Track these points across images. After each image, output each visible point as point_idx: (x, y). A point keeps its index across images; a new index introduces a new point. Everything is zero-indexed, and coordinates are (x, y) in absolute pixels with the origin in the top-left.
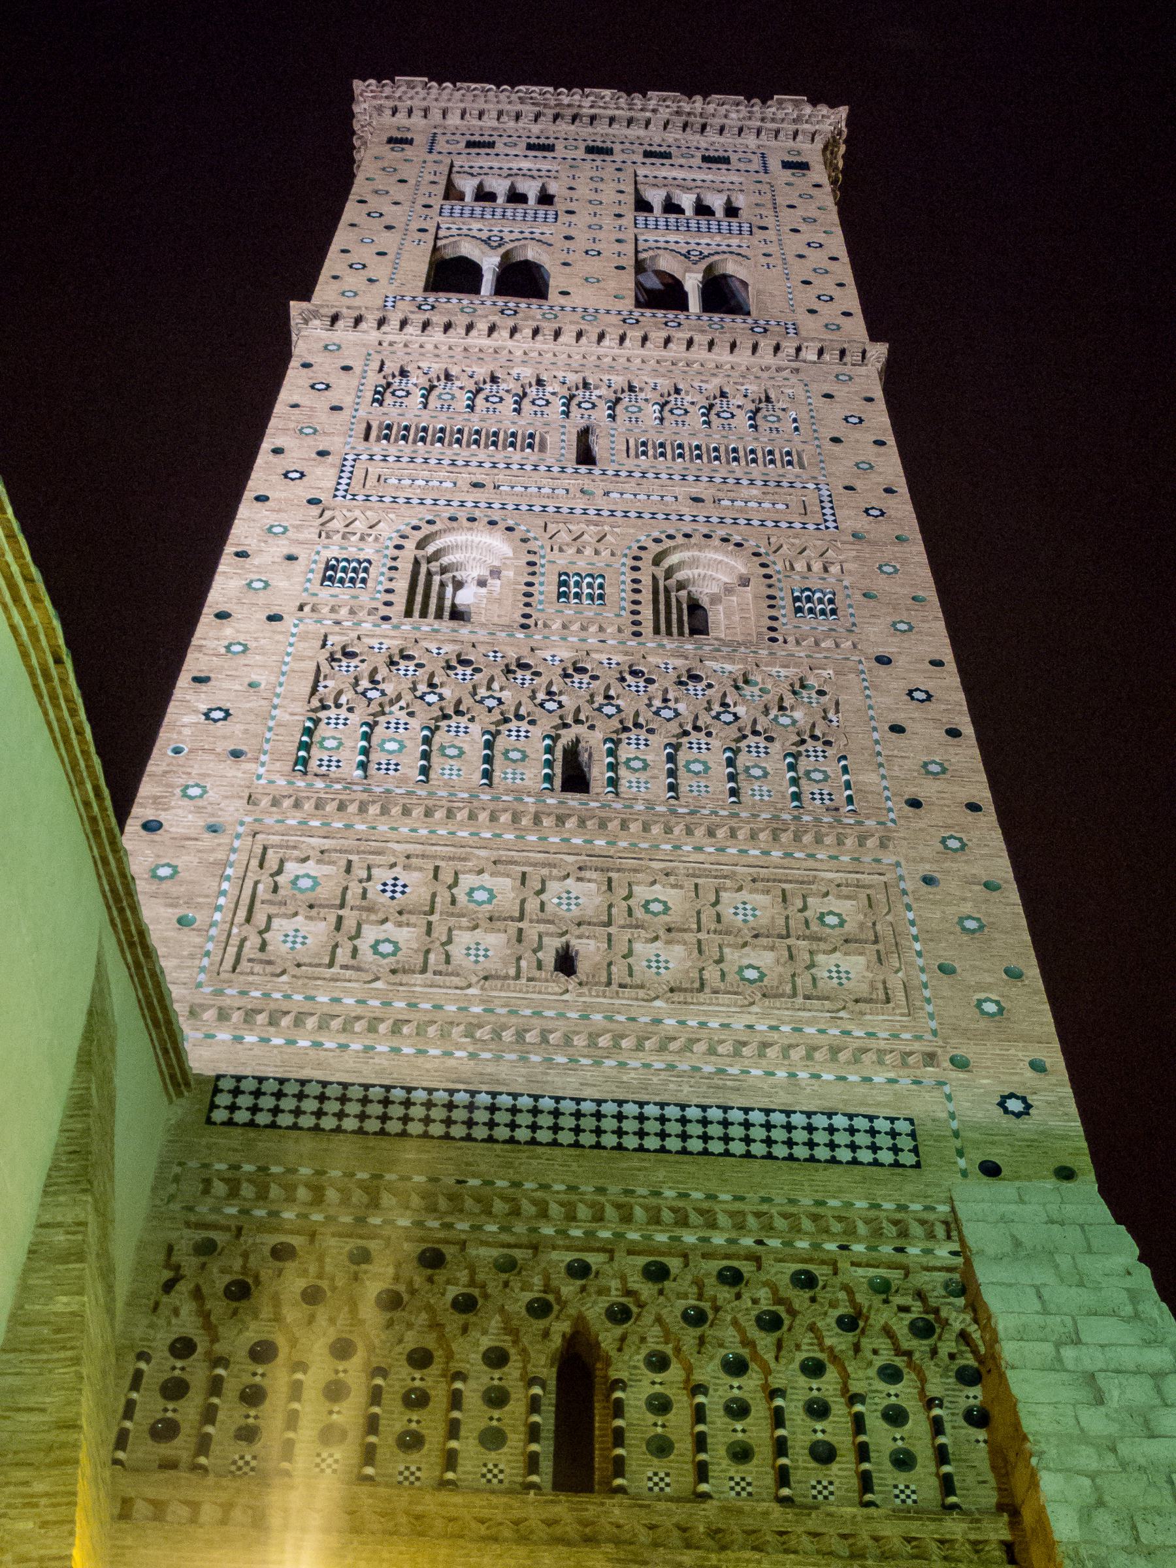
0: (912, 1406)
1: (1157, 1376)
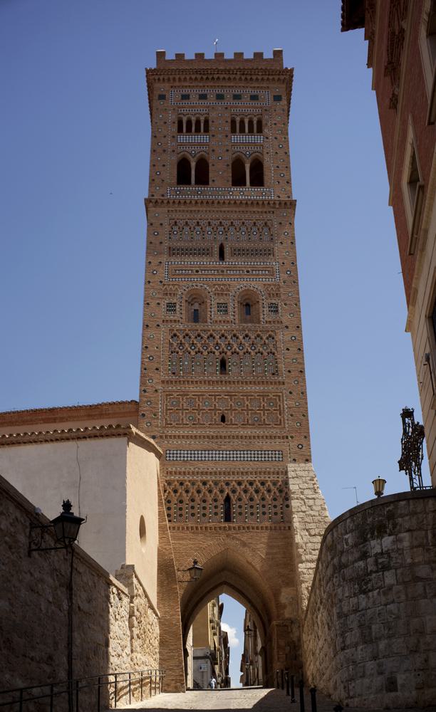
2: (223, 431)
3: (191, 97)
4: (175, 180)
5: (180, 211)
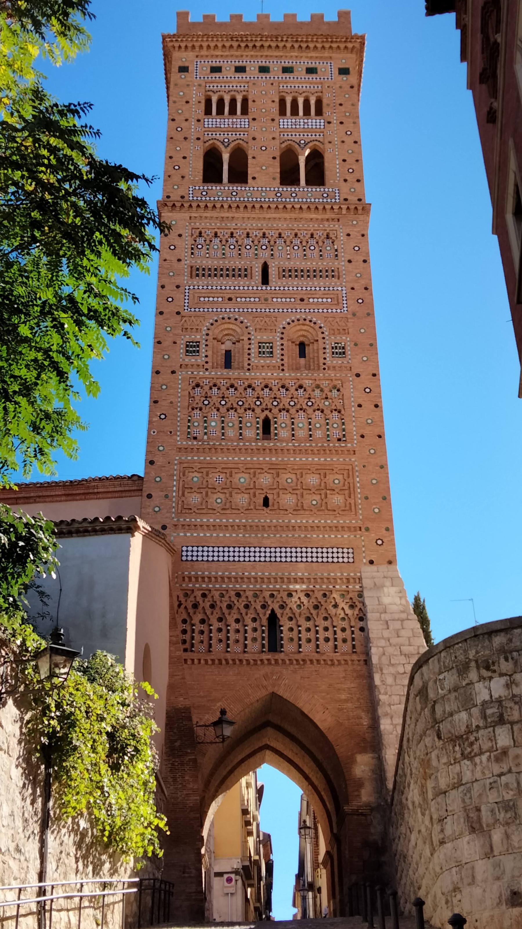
0: (347, 627)
1: (402, 621)
3: (223, 69)
4: (200, 176)
5: (206, 217)
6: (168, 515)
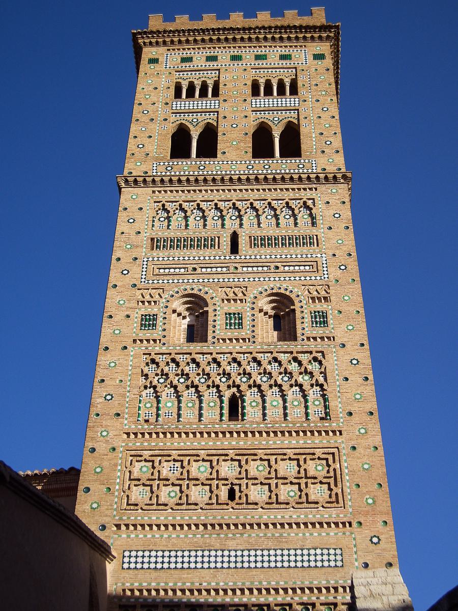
2: (230, 514)
6: (109, 512)
